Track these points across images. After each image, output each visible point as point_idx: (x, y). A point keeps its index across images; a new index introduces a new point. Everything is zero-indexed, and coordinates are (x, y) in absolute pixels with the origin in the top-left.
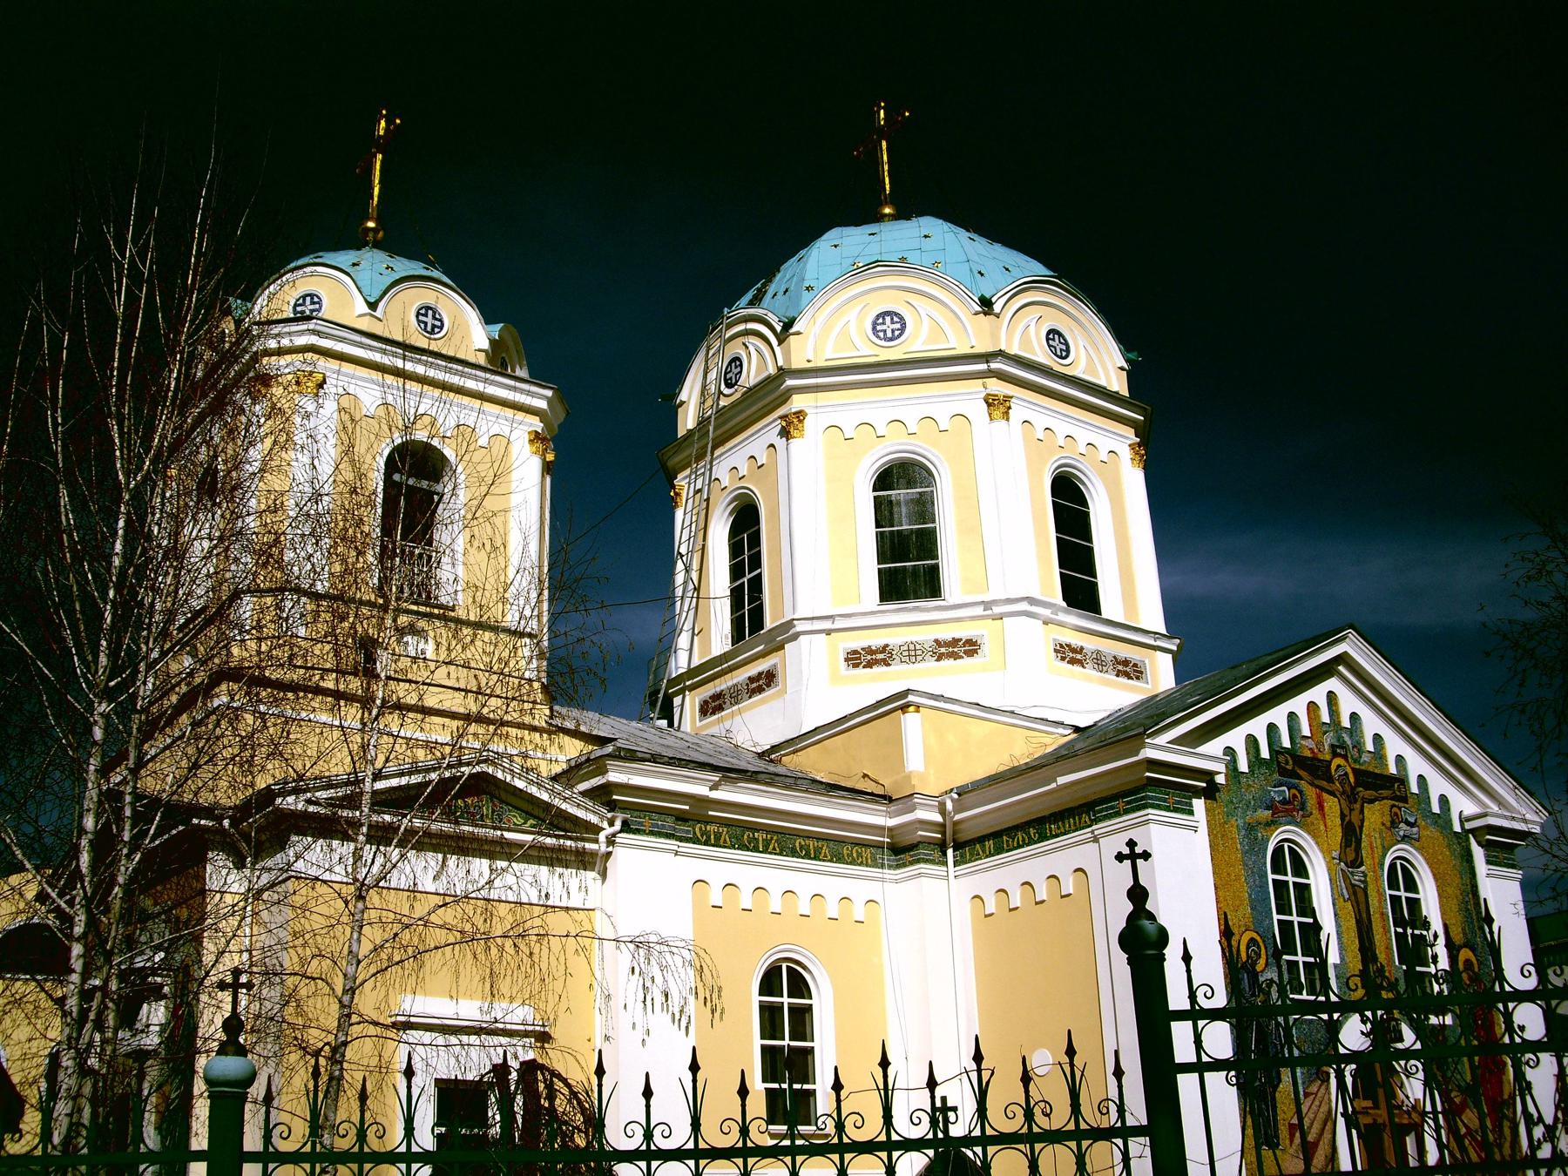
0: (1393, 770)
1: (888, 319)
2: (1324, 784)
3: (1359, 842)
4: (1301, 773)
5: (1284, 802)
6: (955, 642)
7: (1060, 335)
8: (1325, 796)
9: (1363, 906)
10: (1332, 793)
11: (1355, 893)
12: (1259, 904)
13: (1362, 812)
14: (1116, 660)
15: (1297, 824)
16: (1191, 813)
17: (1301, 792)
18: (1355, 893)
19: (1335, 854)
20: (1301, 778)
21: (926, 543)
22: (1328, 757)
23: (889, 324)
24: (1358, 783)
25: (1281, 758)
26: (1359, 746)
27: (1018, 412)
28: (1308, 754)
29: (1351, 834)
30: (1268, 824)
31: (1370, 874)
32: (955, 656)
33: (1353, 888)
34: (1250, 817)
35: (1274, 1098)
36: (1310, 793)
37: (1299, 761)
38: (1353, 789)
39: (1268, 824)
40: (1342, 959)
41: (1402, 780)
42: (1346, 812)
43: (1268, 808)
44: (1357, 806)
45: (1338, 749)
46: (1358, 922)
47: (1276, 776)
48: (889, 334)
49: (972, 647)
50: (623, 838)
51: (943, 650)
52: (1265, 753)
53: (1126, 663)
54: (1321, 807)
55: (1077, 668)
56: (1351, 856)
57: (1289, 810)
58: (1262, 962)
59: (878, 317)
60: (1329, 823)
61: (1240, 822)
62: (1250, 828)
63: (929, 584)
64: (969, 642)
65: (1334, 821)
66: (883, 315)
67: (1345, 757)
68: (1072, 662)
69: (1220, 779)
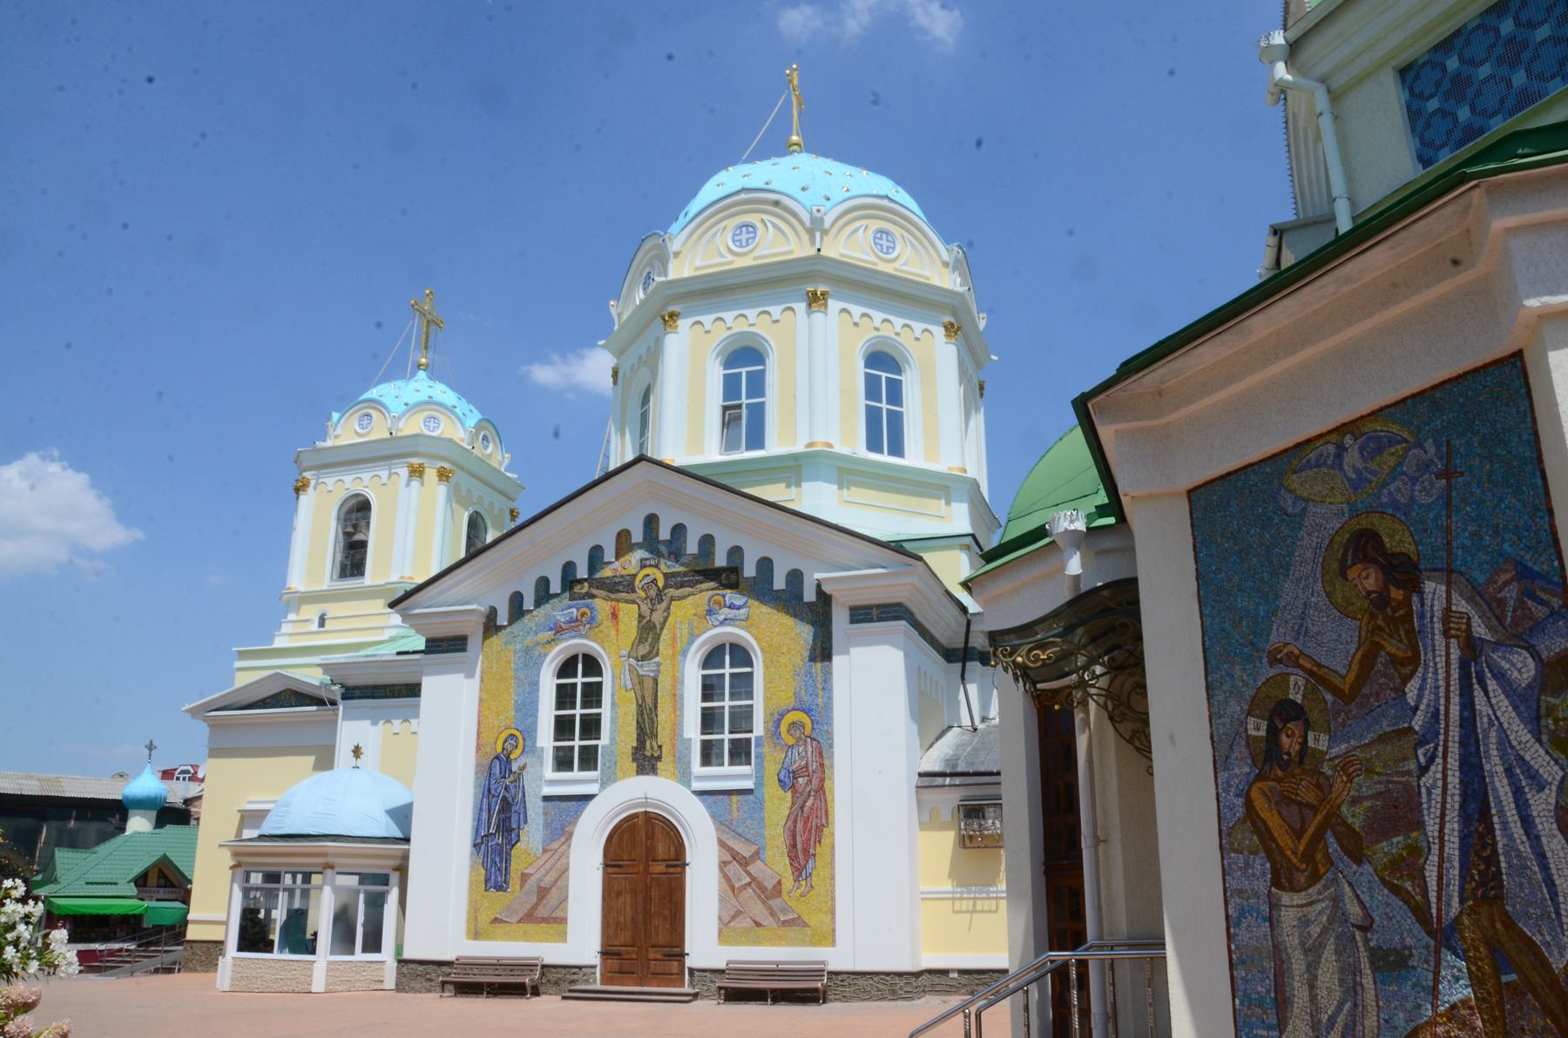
3: (657, 638)
4: (594, 591)
11: (641, 683)
13: (668, 608)
18: (641, 683)
19: (624, 652)
20: (593, 597)
24: (666, 586)
29: (649, 631)
33: (641, 680)
34: (529, 640)
42: (646, 612)
44: (664, 605)
47: (566, 602)
54: (614, 615)
60: (622, 626)
61: (519, 646)
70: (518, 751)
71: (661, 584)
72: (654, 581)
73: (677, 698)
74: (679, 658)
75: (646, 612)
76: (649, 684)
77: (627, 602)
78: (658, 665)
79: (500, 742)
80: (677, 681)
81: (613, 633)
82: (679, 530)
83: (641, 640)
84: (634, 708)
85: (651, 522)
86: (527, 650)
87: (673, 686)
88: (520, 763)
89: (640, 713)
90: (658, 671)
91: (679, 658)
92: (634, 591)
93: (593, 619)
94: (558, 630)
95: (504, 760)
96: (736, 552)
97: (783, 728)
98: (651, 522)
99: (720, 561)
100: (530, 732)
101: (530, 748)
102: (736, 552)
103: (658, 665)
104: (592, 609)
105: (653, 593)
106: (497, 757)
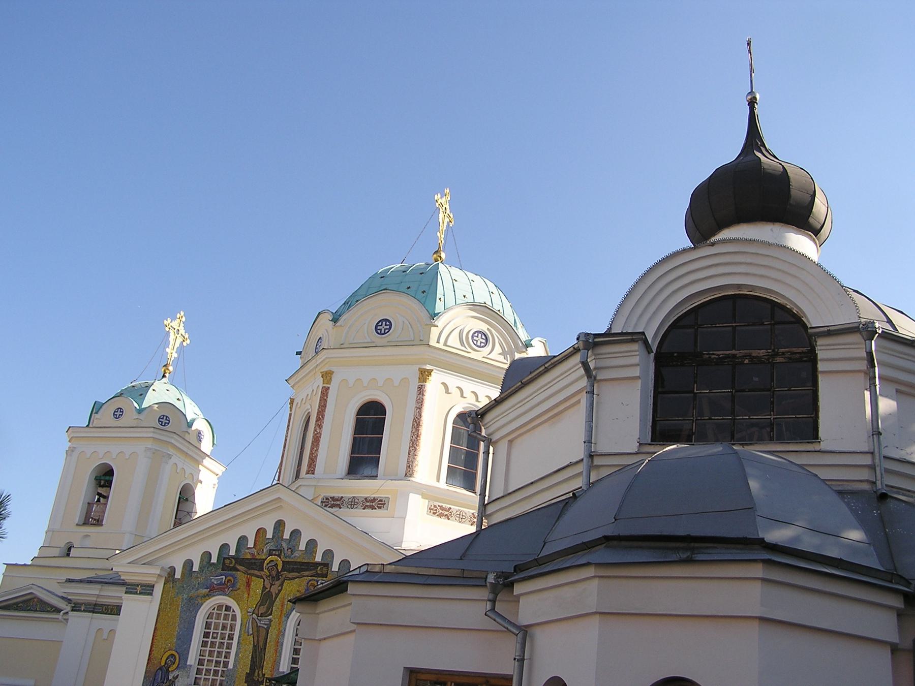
4: (239, 567)
11: (258, 631)
13: (282, 585)
15: (225, 595)
18: (258, 631)
20: (238, 570)
28: (249, 557)
29: (267, 599)
30: (204, 596)
34: (193, 593)
39: (204, 596)
41: (326, 565)
42: (268, 586)
46: (254, 646)
47: (220, 571)
50: (71, 613)
54: (248, 585)
56: (262, 610)
60: (252, 593)
70: (175, 666)
71: (280, 568)
72: (276, 565)
73: (279, 645)
74: (284, 619)
75: (268, 586)
76: (263, 633)
77: (257, 576)
78: (270, 621)
80: (281, 633)
81: (246, 595)
82: (296, 533)
83: (262, 602)
85: (280, 525)
86: (190, 599)
87: (278, 636)
88: (176, 673)
90: (269, 625)
91: (284, 619)
92: (263, 570)
93: (234, 585)
94: (213, 590)
95: (165, 670)
96: (329, 553)
98: (280, 525)
99: (318, 558)
100: (184, 655)
101: (182, 665)
102: (329, 553)
103: (270, 621)
104: (235, 578)
105: (274, 573)
106: (160, 669)
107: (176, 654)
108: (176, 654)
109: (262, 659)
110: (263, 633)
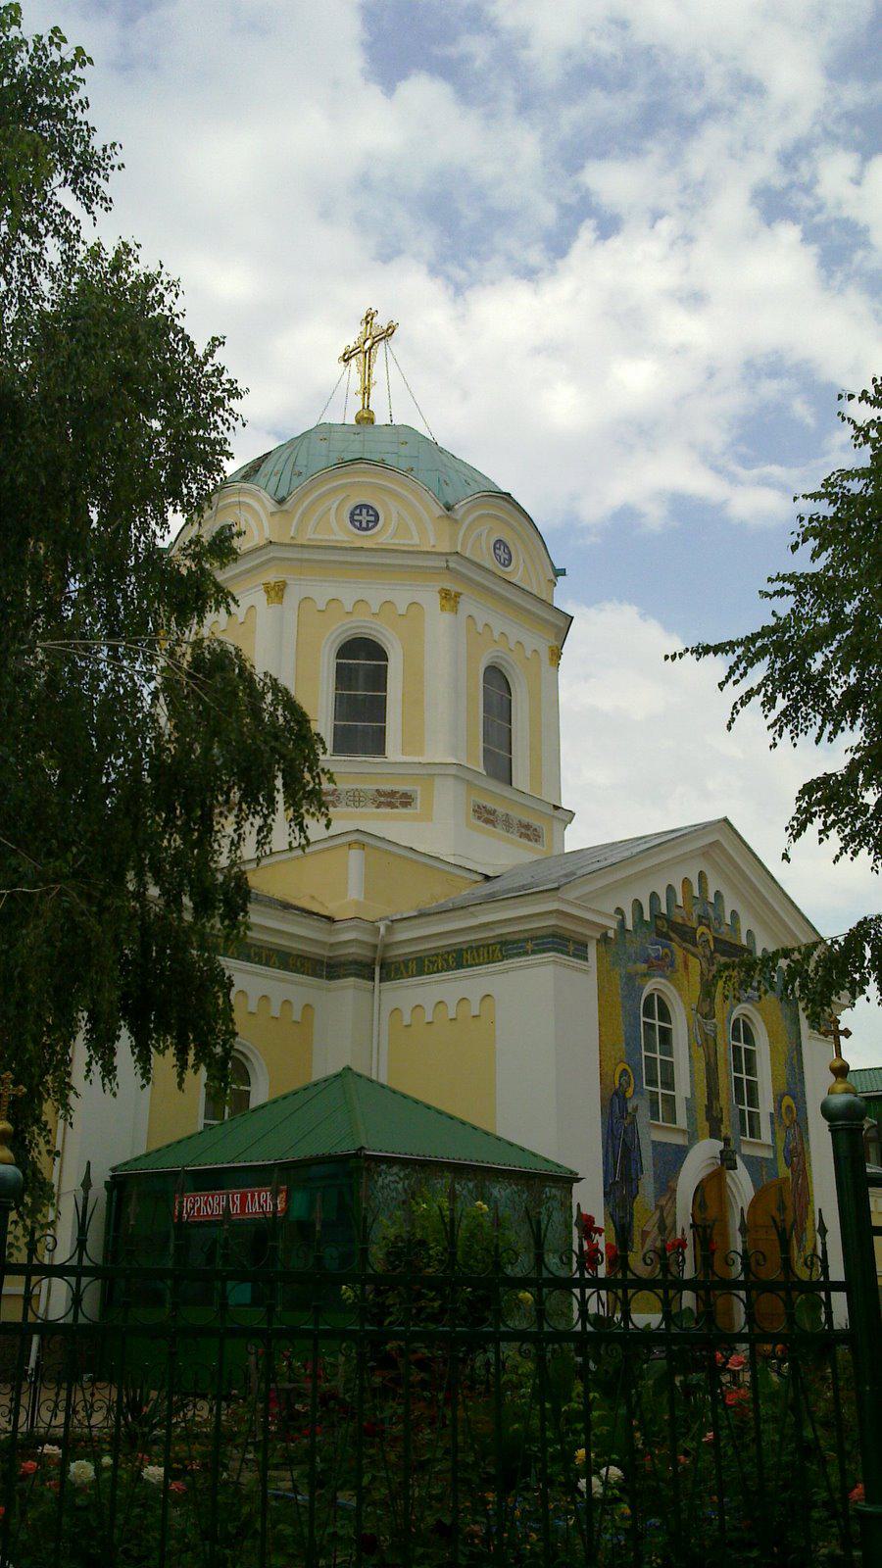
0: (744, 942)
1: (364, 511)
2: (689, 946)
4: (673, 935)
5: (657, 958)
6: (393, 794)
7: (506, 546)
8: (690, 957)
9: (712, 1053)
10: (695, 955)
11: (706, 1040)
12: (632, 1041)
14: (521, 825)
15: (666, 977)
16: (586, 959)
17: (672, 952)
18: (706, 1040)
19: (694, 1006)
20: (671, 940)
21: (377, 709)
22: (695, 925)
23: (365, 517)
24: (716, 951)
25: (659, 923)
26: (719, 918)
27: (467, 606)
28: (680, 921)
31: (720, 1026)
32: (391, 805)
35: (632, 1208)
36: (679, 953)
37: (673, 926)
38: (712, 953)
39: (645, 975)
40: (693, 1094)
42: (706, 972)
43: (646, 962)
45: (703, 919)
46: (707, 1064)
47: (654, 935)
48: (364, 525)
49: (406, 800)
51: (382, 799)
52: (647, 917)
53: (528, 827)
54: (686, 966)
55: (489, 827)
56: (706, 1009)
57: (661, 965)
58: (630, 1091)
59: (357, 507)
62: (630, 977)
63: (376, 744)
64: (405, 795)
65: (696, 978)
66: (360, 507)
67: (708, 927)
68: (487, 821)
69: (611, 934)
79: (617, 1076)
84: (703, 1066)
89: (708, 1070)
97: (783, 1108)
106: (616, 1093)
107: (630, 1071)
108: (630, 1071)
109: (717, 1084)
110: (711, 1044)
